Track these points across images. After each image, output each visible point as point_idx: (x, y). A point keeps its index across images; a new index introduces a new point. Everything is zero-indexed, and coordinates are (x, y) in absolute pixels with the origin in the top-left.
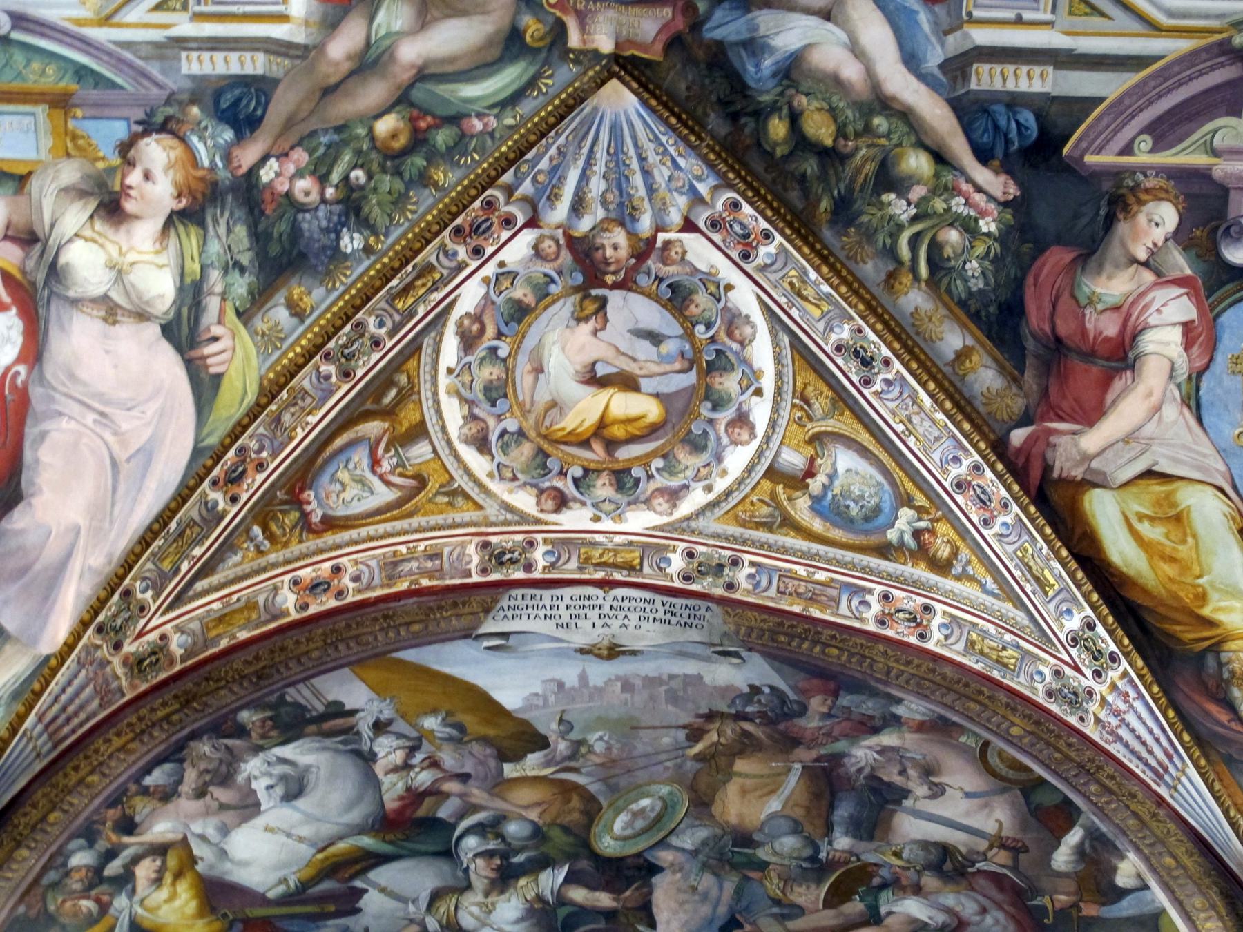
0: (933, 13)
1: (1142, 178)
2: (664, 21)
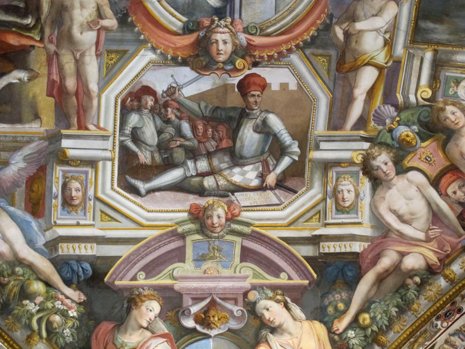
1: (142, 290)
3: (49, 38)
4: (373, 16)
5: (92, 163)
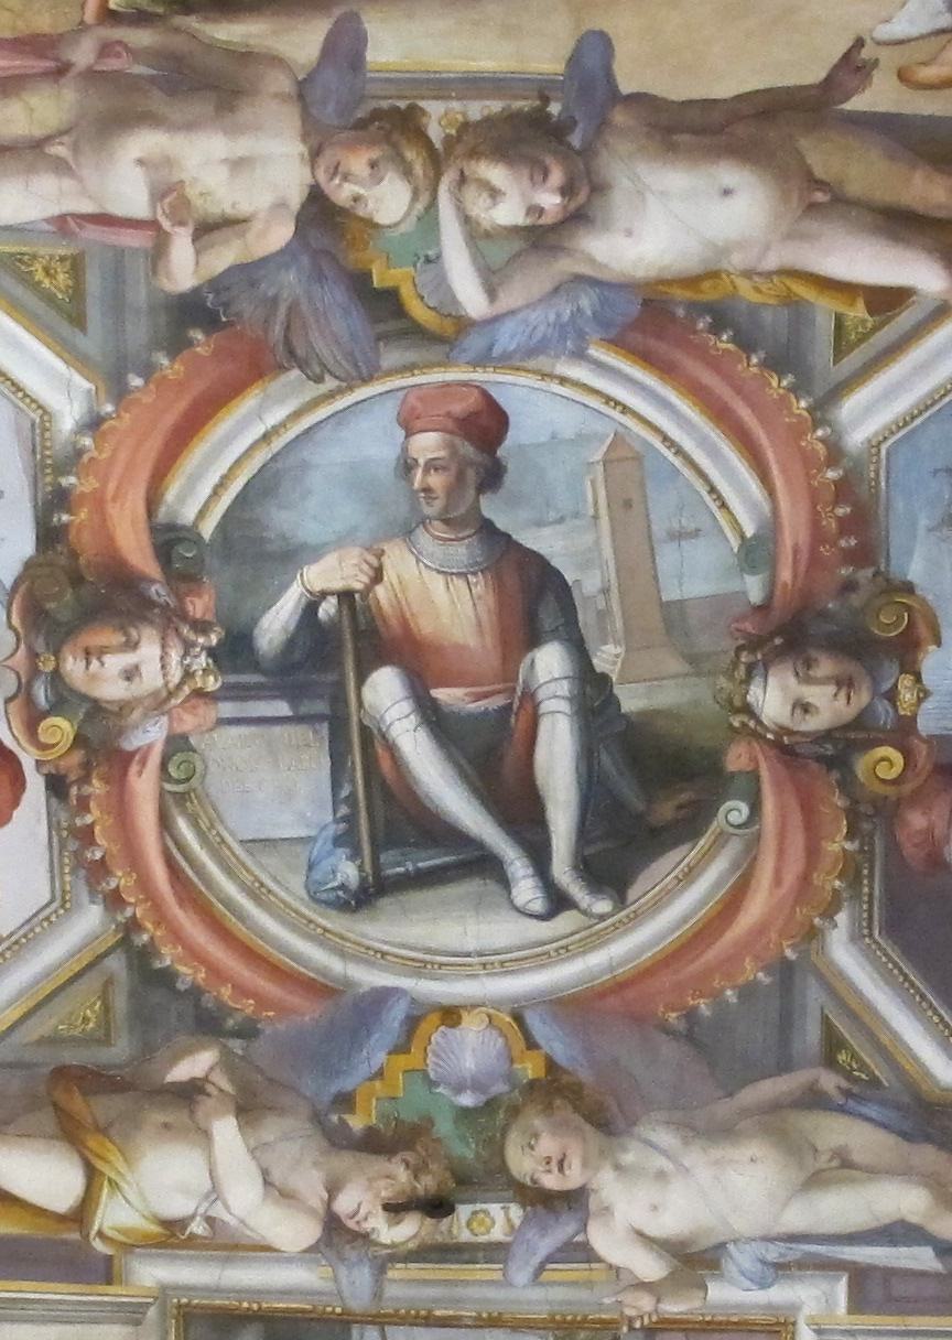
3: (120, 42)
4: (265, 1173)
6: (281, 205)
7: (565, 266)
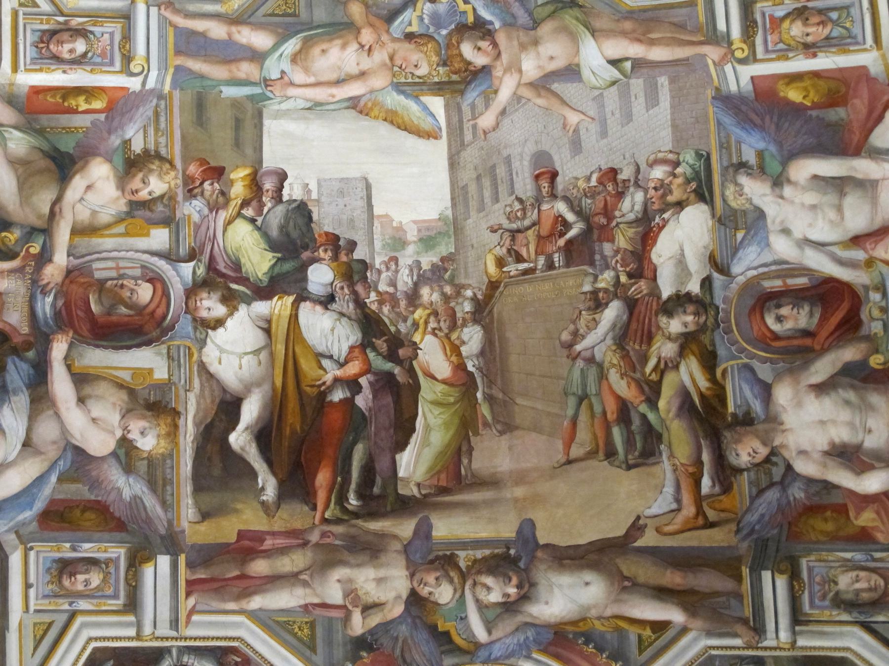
0: (31, 522)
2: (18, 328)
3: (330, 531)
5: (133, 605)
6: (398, 597)
7: (520, 619)
